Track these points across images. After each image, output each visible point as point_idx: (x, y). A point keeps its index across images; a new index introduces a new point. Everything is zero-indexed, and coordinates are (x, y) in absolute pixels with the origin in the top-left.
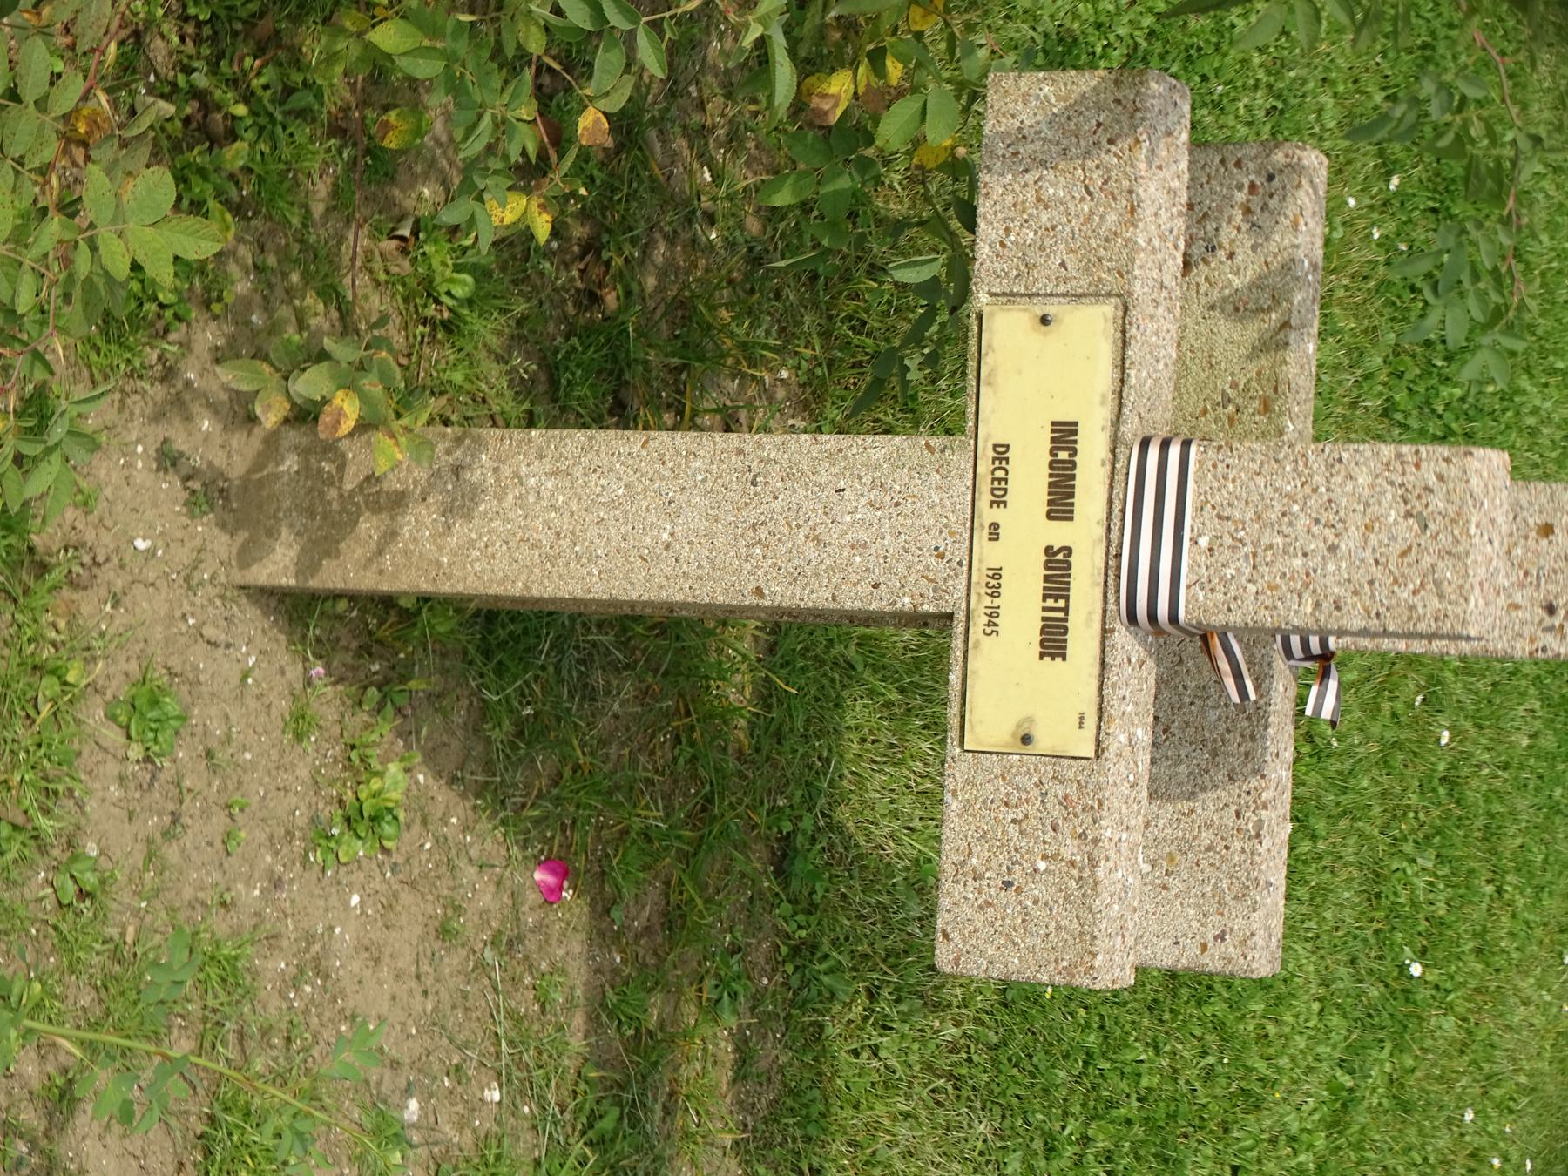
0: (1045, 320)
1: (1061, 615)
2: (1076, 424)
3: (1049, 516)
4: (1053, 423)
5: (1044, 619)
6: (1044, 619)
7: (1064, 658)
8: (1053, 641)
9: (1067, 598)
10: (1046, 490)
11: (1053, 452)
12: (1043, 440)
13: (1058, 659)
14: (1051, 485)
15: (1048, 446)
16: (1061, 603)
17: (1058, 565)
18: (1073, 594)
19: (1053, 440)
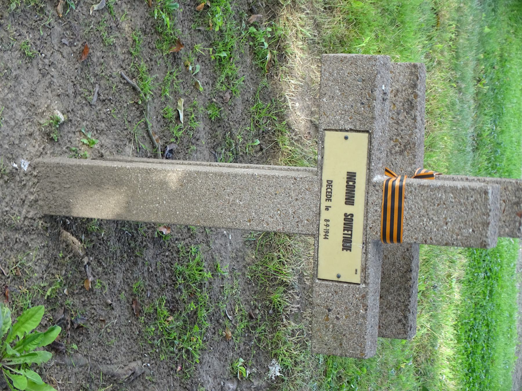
0: (346, 138)
1: (350, 236)
2: (355, 173)
4: (348, 172)
5: (344, 237)
6: (344, 237)
7: (350, 251)
9: (352, 231)
10: (345, 194)
11: (347, 182)
15: (346, 180)
16: (350, 232)
17: (349, 220)
18: (353, 230)
19: (347, 178)
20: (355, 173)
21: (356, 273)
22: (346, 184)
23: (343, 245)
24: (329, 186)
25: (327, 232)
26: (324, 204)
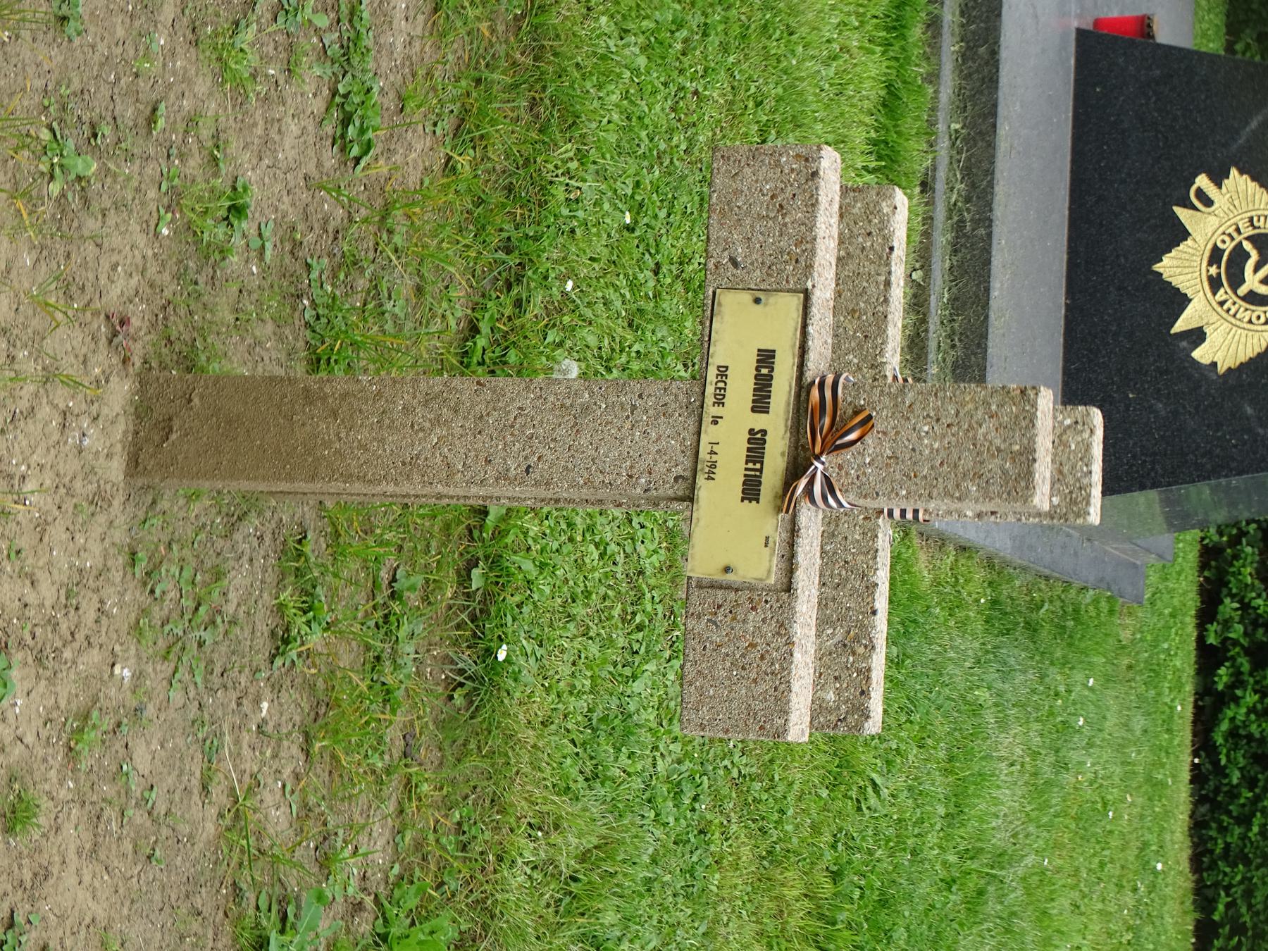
1: (758, 473)
2: (774, 351)
3: (753, 410)
4: (759, 350)
5: (745, 476)
6: (745, 476)
7: (758, 502)
9: (762, 463)
10: (752, 393)
11: (757, 369)
12: (753, 359)
13: (754, 502)
14: (755, 390)
15: (755, 365)
16: (758, 466)
18: (765, 460)
19: (758, 361)
20: (774, 351)
21: (766, 546)
23: (743, 491)
24: (722, 376)
25: (713, 465)
26: (711, 410)
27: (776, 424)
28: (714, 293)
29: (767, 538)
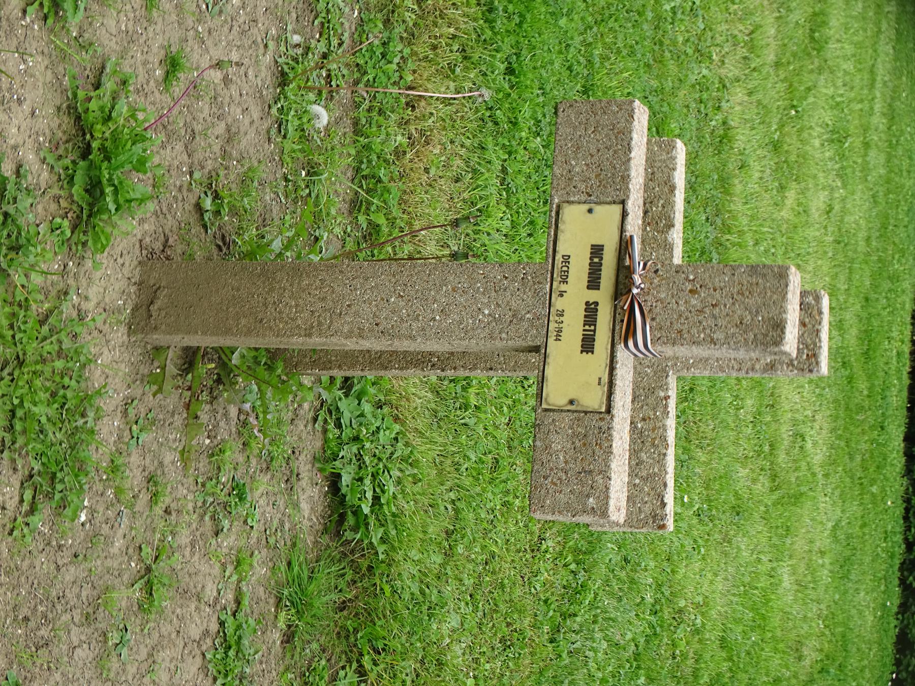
3: (588, 288)
7: (593, 353)
8: (588, 345)
9: (595, 325)
10: (587, 275)
11: (591, 259)
14: (589, 273)
15: (589, 256)
16: (592, 328)
17: (591, 310)
19: (591, 253)
22: (589, 261)
27: (603, 296)
28: (559, 207)
29: (600, 379)
